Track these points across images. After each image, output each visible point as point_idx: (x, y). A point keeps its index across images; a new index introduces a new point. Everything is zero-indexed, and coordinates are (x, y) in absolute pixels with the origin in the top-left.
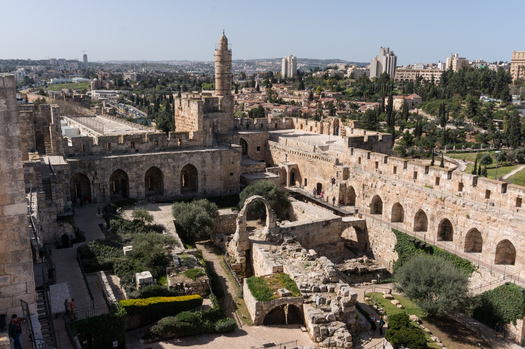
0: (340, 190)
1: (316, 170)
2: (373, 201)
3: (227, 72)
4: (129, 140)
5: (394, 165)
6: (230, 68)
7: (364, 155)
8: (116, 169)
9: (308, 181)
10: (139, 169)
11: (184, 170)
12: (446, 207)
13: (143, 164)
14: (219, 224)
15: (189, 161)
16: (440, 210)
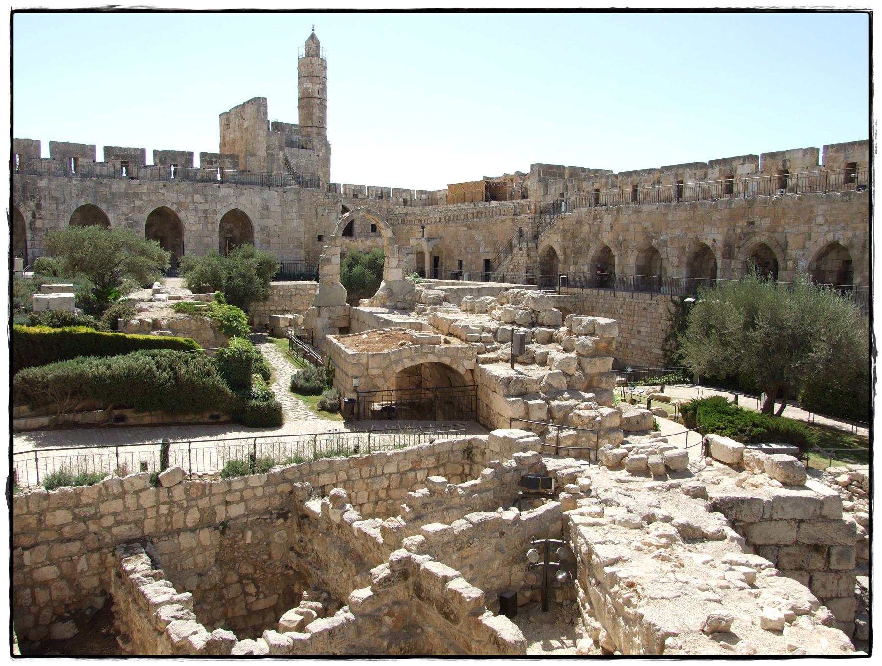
0: (528, 255)
1: (478, 237)
2: (593, 260)
3: (318, 96)
4: (117, 156)
5: (632, 183)
6: (324, 90)
7: (570, 185)
8: (83, 203)
9: (464, 263)
10: (133, 210)
11: (228, 226)
12: (757, 222)
13: (141, 199)
14: (288, 303)
15: (236, 203)
16: (745, 231)
